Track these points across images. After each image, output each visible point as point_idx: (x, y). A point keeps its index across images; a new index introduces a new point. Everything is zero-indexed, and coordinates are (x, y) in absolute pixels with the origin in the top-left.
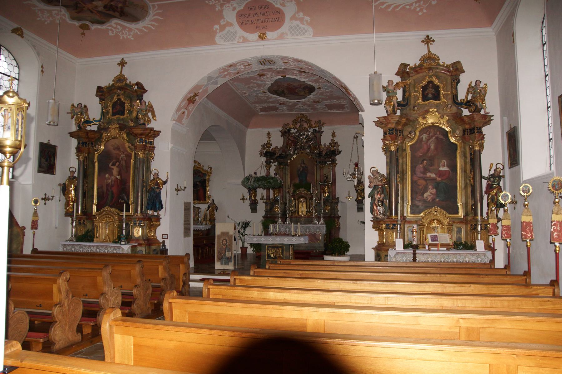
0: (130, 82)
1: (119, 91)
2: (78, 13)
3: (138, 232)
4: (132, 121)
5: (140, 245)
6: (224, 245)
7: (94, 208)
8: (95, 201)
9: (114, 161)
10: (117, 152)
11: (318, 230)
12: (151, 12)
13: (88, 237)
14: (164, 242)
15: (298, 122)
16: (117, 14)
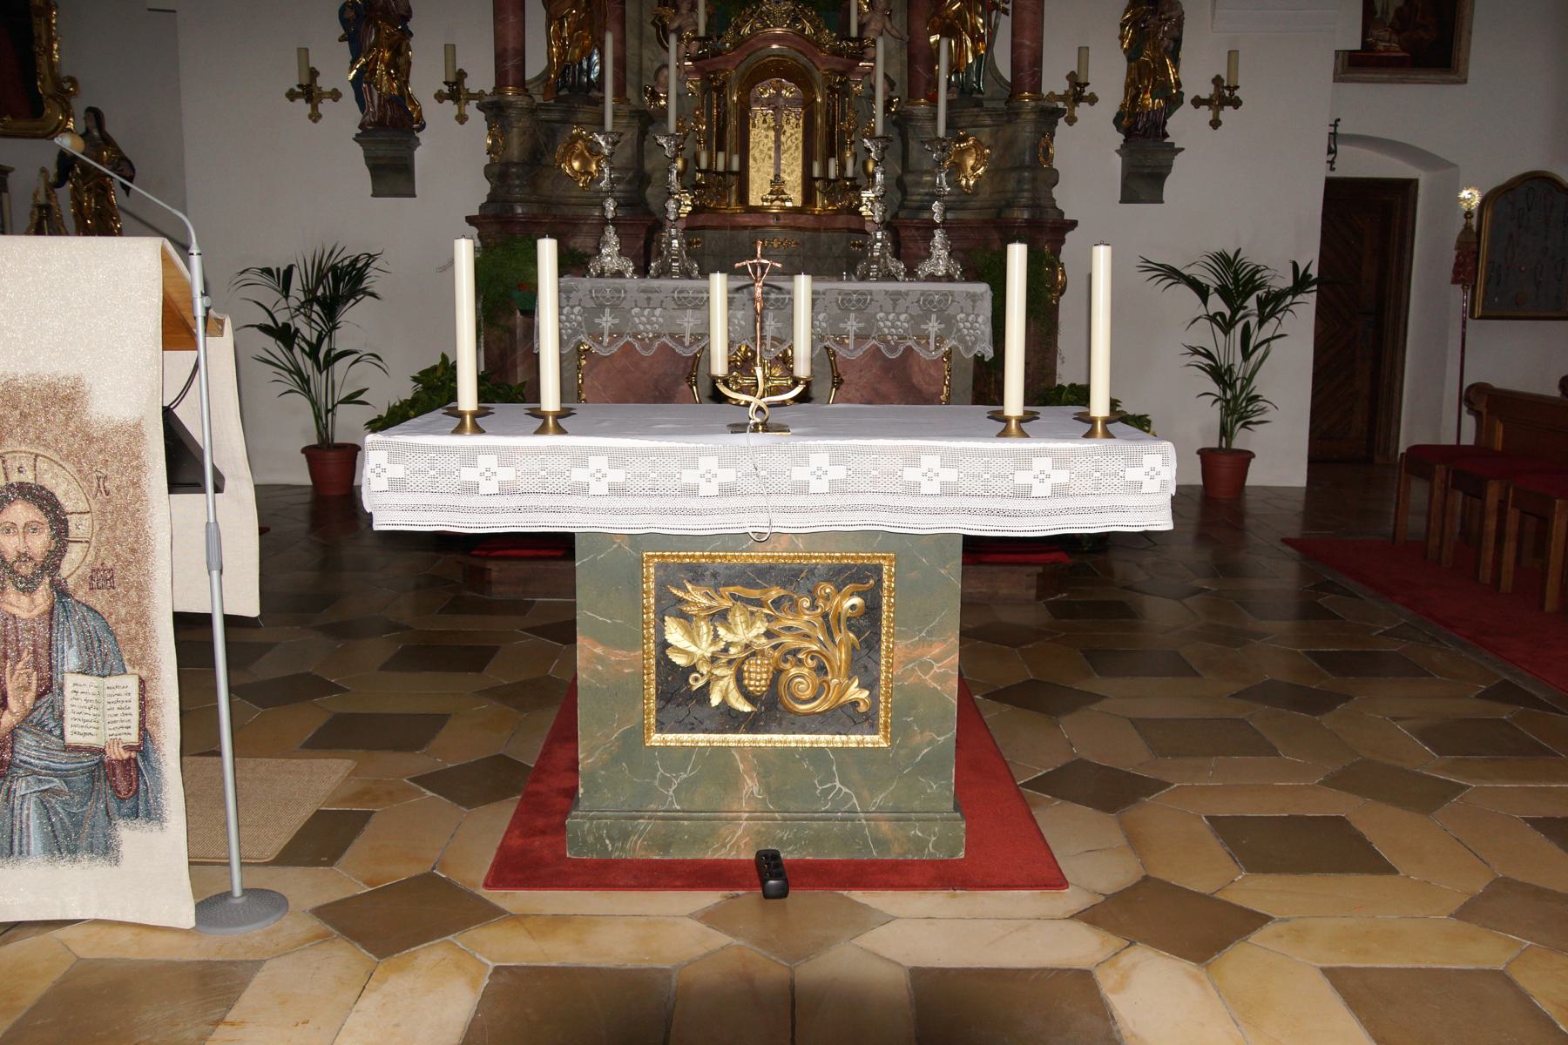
11: (933, 327)
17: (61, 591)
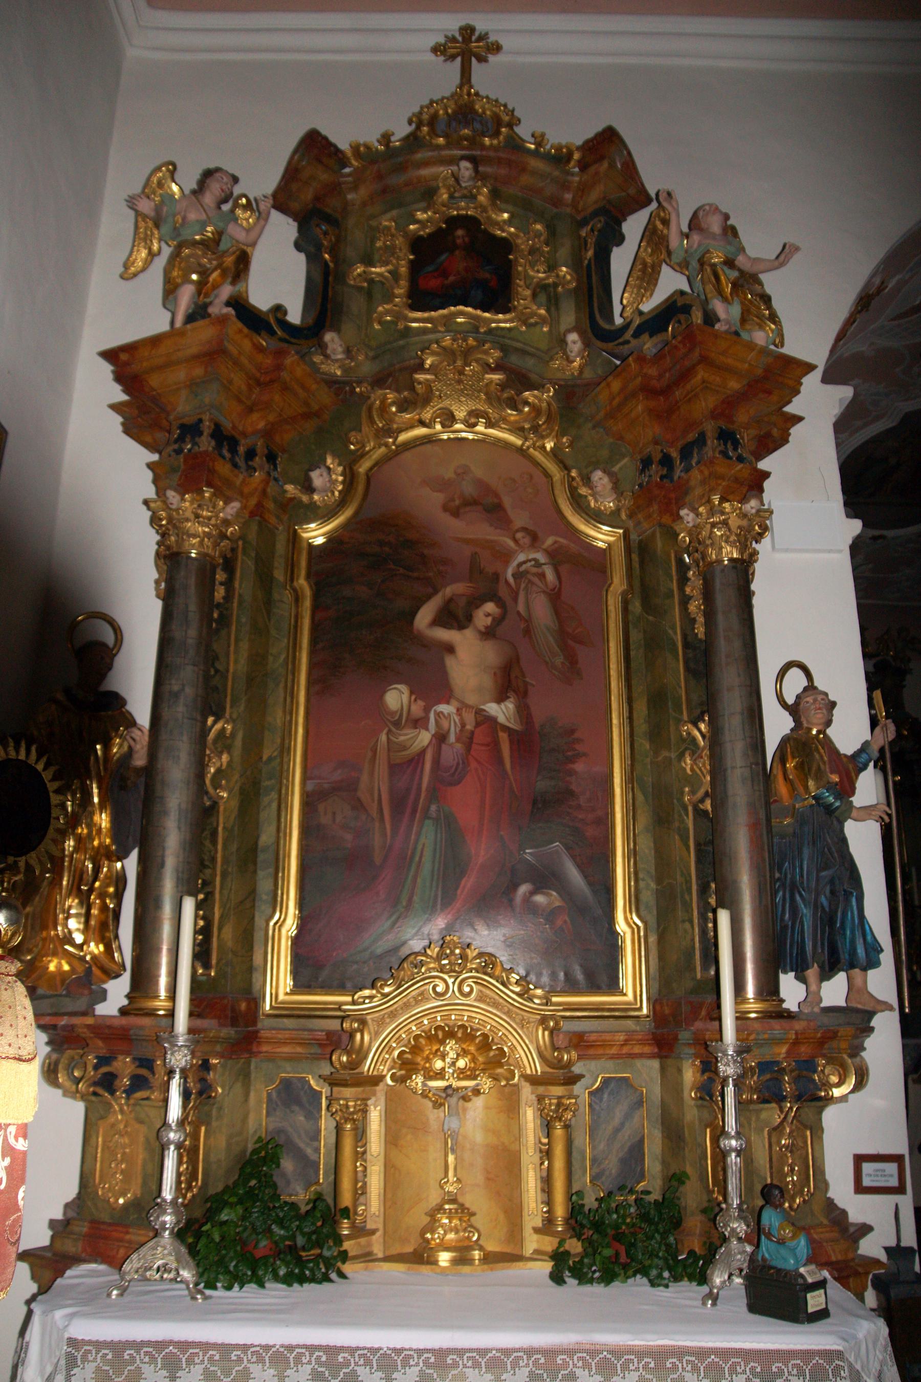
9: (456, 589)
10: (477, 529)
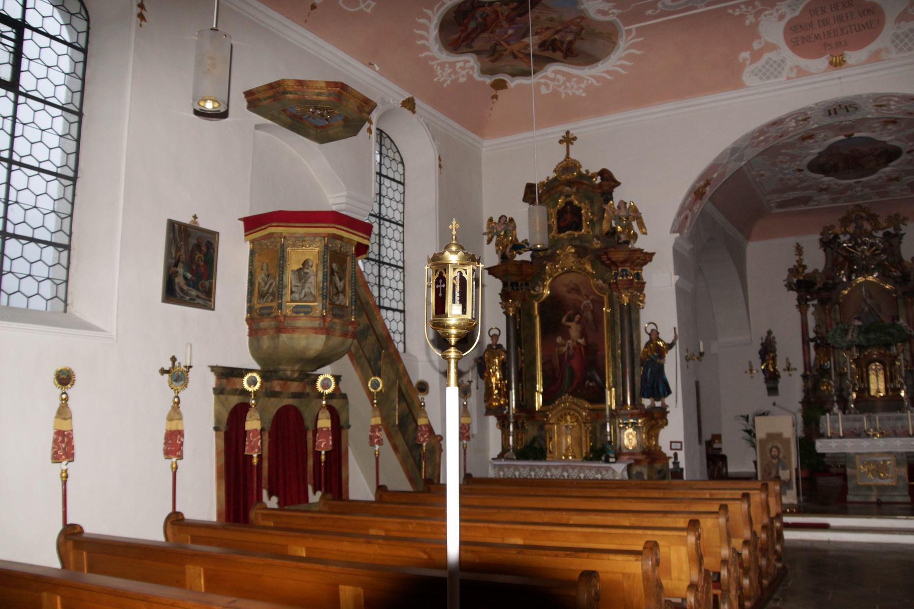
0: (587, 171)
1: (567, 188)
2: (493, 61)
3: (629, 439)
4: (598, 239)
5: (638, 462)
6: (772, 457)
7: (539, 400)
8: (539, 387)
12: (622, 43)
13: (534, 450)
14: (676, 455)
15: (851, 222)
16: (559, 54)
17: (779, 459)
